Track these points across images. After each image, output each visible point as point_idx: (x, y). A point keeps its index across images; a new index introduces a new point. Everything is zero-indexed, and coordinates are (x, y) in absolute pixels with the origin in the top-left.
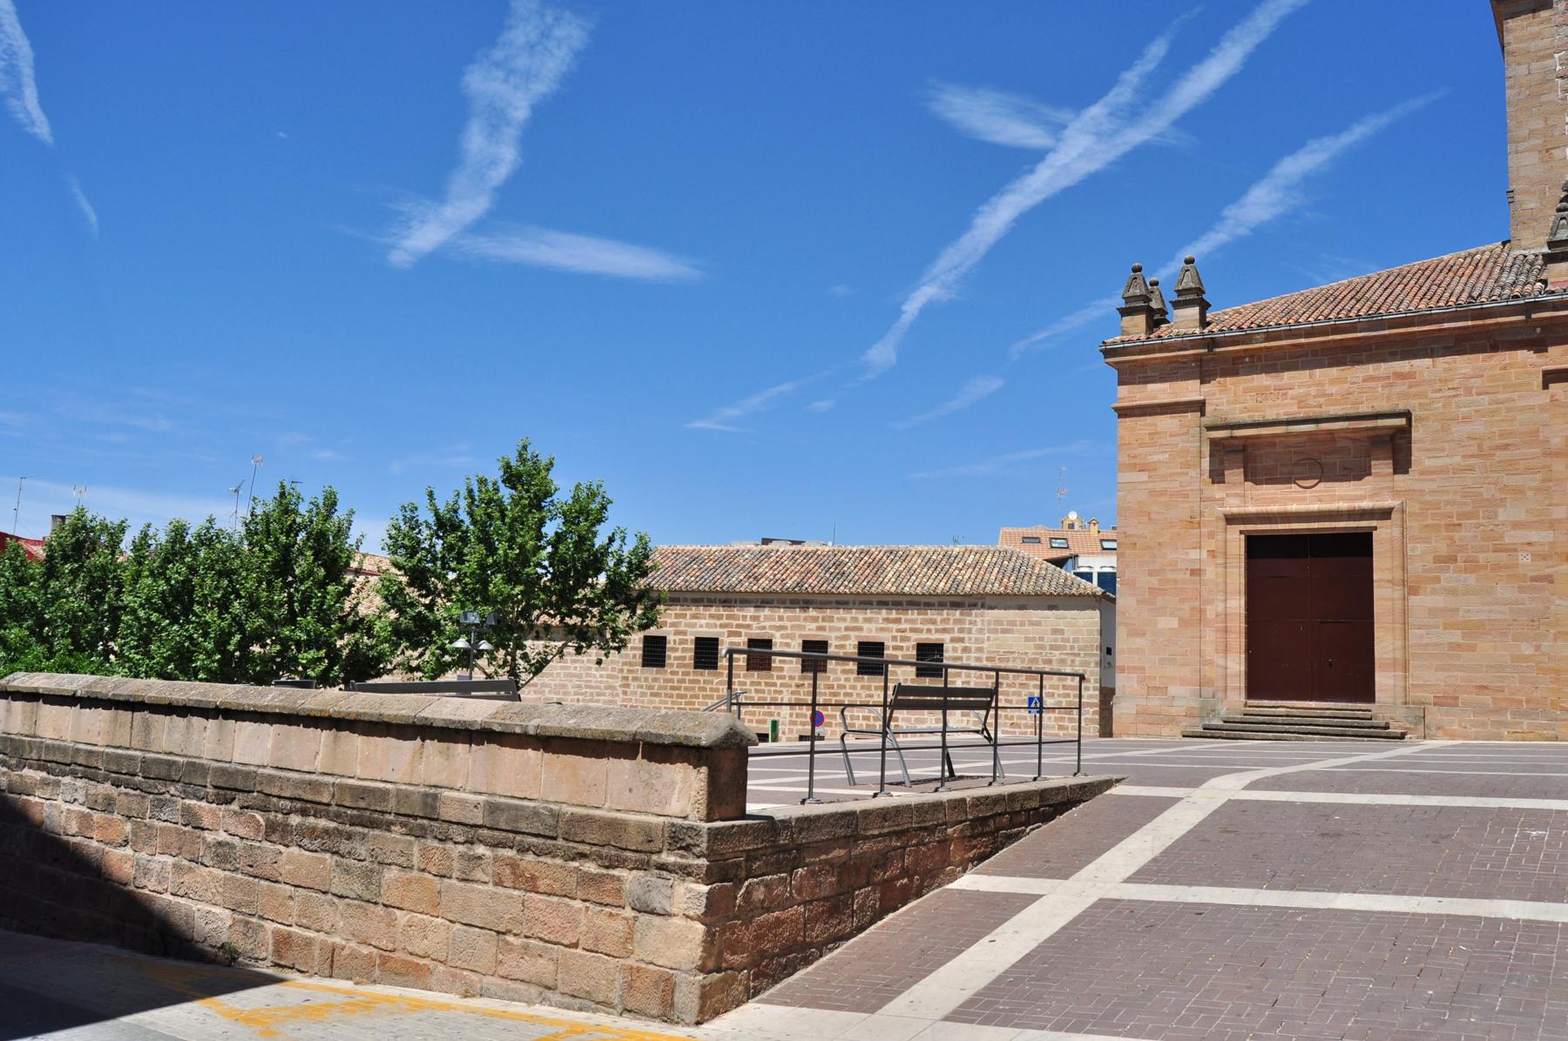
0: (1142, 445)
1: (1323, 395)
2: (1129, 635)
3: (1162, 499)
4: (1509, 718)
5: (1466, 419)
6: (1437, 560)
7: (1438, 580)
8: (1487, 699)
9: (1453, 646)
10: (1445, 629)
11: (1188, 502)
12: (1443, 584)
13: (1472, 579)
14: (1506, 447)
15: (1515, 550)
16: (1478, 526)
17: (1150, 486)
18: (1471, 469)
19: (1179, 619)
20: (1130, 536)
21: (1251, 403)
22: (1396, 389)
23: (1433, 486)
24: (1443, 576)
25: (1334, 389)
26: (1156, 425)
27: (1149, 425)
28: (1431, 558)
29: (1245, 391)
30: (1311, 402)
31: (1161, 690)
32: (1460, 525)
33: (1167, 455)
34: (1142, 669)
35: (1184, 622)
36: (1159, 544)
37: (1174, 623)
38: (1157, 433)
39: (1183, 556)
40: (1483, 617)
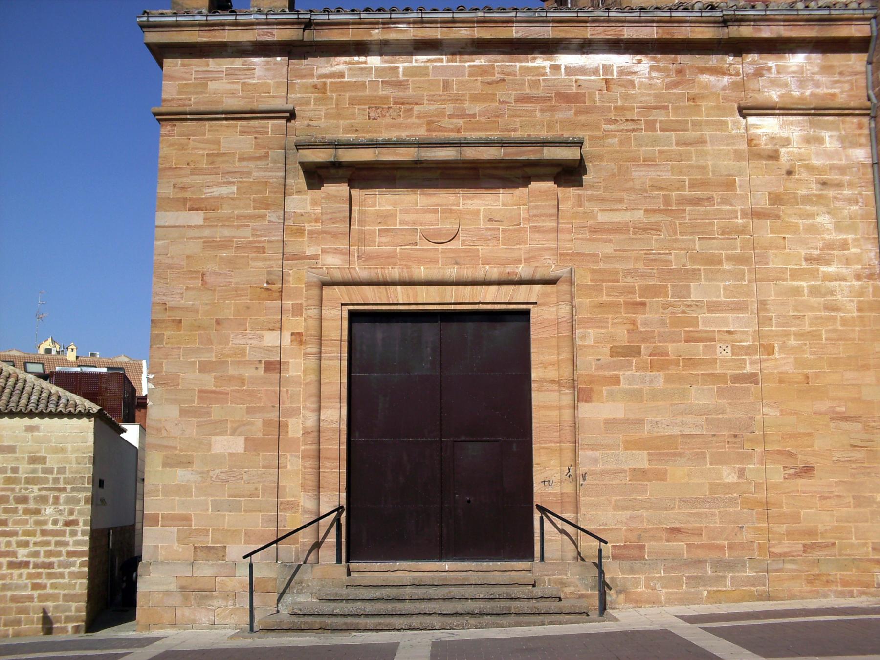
0: (195, 171)
1: (462, 116)
4: (709, 572)
5: (649, 162)
6: (615, 352)
7: (616, 380)
8: (680, 545)
9: (640, 474)
10: (626, 449)
11: (265, 259)
12: (624, 385)
13: (659, 380)
15: (713, 340)
16: (665, 307)
17: (207, 232)
18: (655, 228)
19: (246, 440)
20: (172, 308)
21: (360, 119)
22: (559, 116)
23: (608, 249)
24: (624, 375)
25: (476, 108)
26: (218, 143)
27: (208, 142)
28: (607, 350)
29: (353, 102)
30: (446, 122)
32: (643, 304)
33: (234, 189)
34: (186, 519)
35: (252, 444)
36: (218, 322)
37: (237, 445)
39: (255, 342)
40: (676, 431)
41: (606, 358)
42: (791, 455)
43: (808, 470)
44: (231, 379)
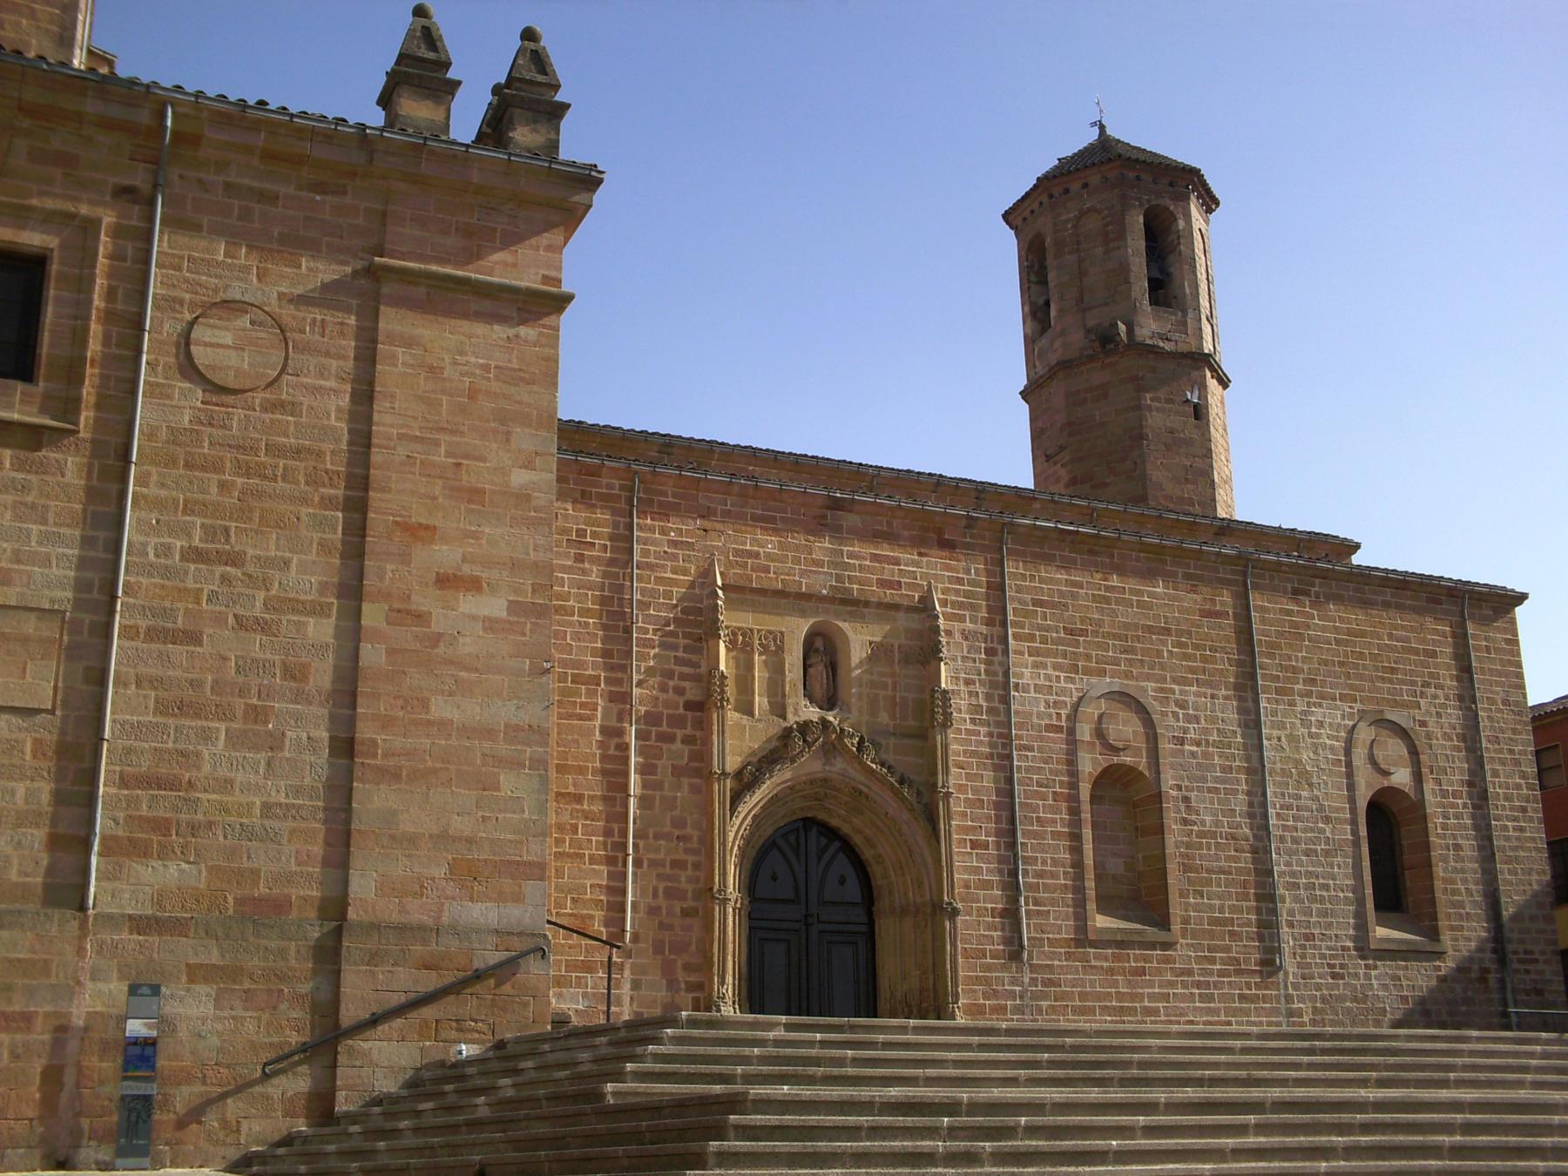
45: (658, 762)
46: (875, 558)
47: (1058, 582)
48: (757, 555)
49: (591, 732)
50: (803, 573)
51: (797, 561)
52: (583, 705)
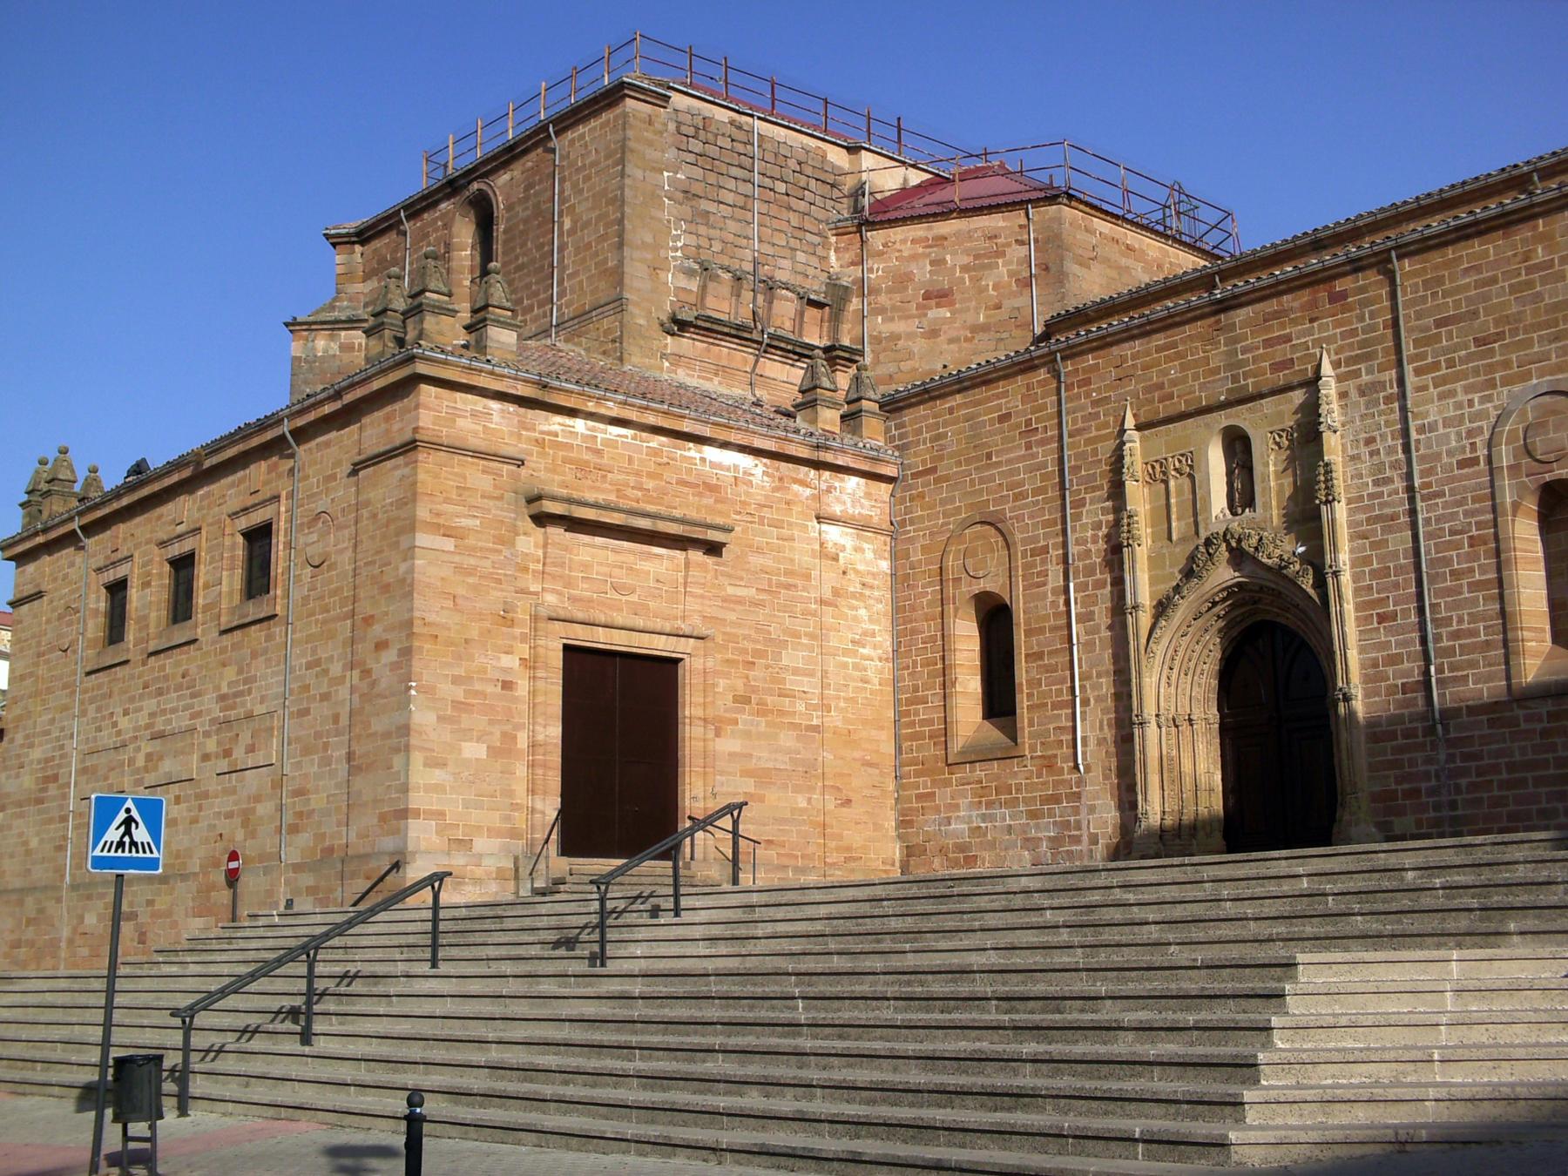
0: (447, 501)
1: (640, 489)
2: (426, 765)
3: (471, 580)
5: (759, 550)
6: (736, 699)
11: (502, 590)
14: (788, 587)
16: (767, 667)
17: (457, 558)
18: (759, 604)
20: (430, 624)
21: (569, 478)
22: (705, 501)
23: (732, 617)
24: (742, 717)
25: (650, 484)
27: (456, 474)
29: (565, 461)
30: (629, 492)
31: (464, 844)
32: (754, 663)
34: (442, 814)
36: (467, 641)
38: (464, 488)
39: (494, 663)
40: (770, 765)
41: (730, 704)
42: (838, 789)
43: (848, 802)
44: (477, 694)
45: (1096, 609)
46: (1268, 343)
47: (1467, 287)
48: (1160, 386)
49: (1045, 595)
50: (1202, 387)
51: (1196, 377)
52: (1039, 574)
